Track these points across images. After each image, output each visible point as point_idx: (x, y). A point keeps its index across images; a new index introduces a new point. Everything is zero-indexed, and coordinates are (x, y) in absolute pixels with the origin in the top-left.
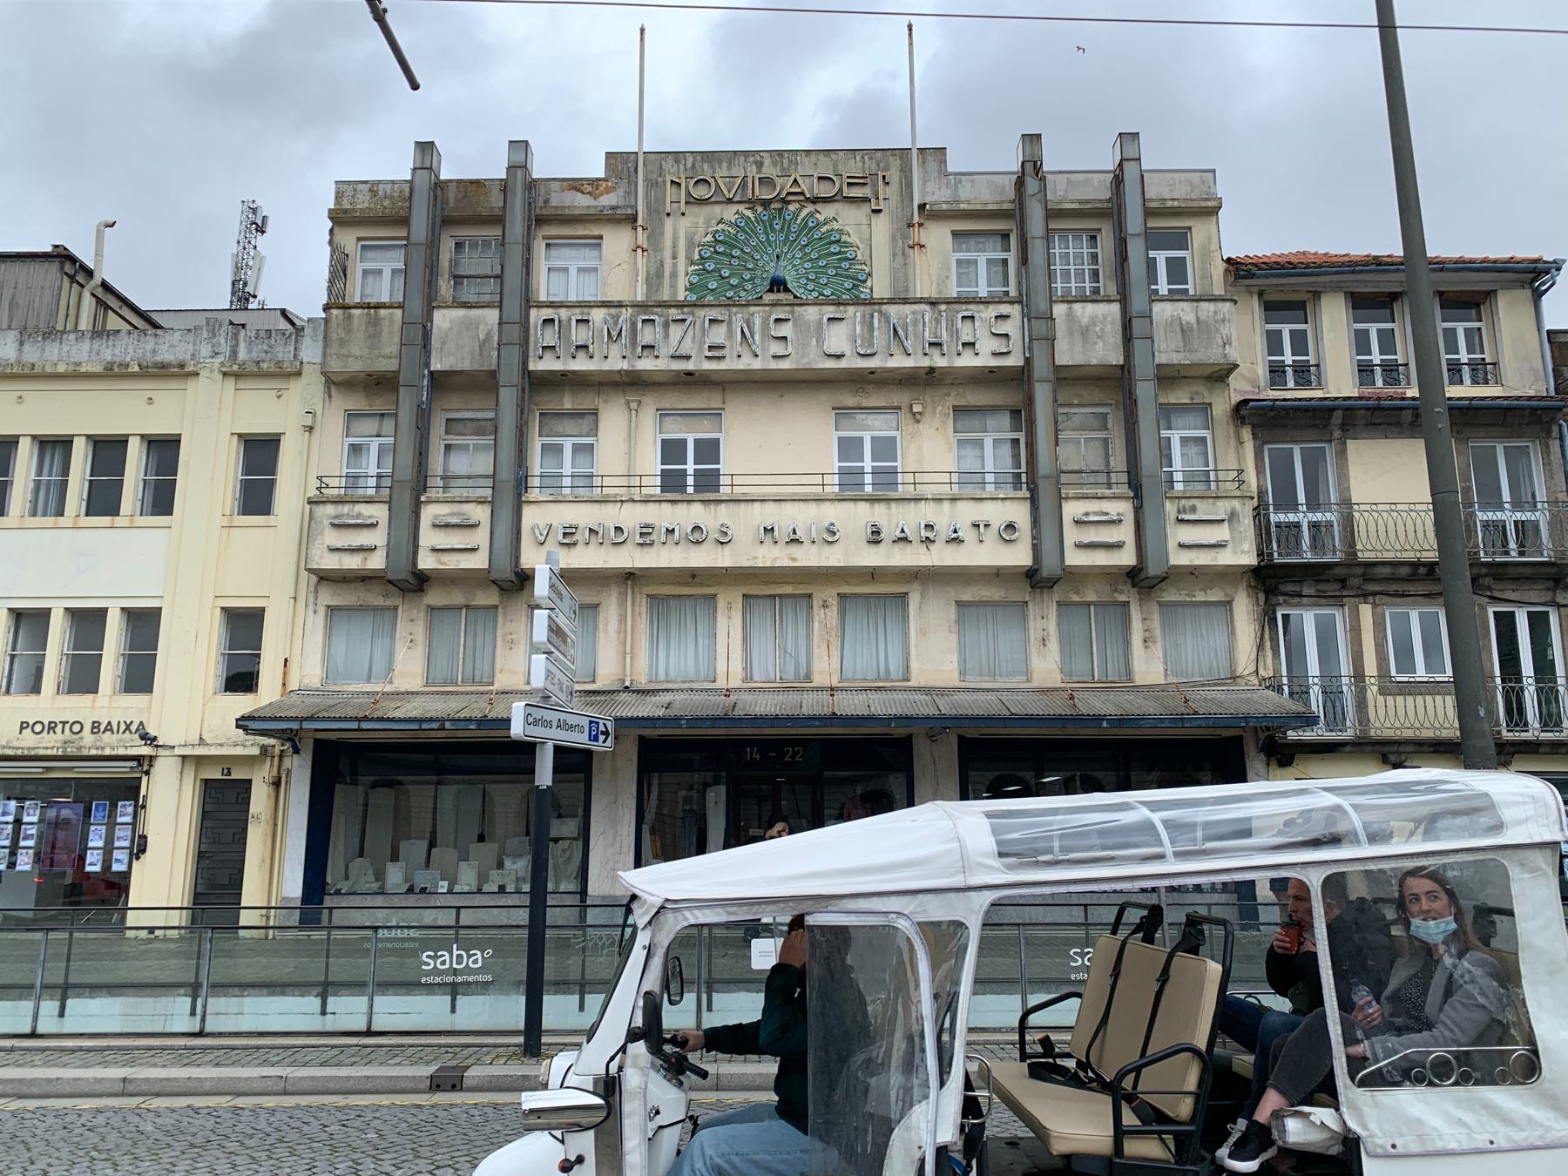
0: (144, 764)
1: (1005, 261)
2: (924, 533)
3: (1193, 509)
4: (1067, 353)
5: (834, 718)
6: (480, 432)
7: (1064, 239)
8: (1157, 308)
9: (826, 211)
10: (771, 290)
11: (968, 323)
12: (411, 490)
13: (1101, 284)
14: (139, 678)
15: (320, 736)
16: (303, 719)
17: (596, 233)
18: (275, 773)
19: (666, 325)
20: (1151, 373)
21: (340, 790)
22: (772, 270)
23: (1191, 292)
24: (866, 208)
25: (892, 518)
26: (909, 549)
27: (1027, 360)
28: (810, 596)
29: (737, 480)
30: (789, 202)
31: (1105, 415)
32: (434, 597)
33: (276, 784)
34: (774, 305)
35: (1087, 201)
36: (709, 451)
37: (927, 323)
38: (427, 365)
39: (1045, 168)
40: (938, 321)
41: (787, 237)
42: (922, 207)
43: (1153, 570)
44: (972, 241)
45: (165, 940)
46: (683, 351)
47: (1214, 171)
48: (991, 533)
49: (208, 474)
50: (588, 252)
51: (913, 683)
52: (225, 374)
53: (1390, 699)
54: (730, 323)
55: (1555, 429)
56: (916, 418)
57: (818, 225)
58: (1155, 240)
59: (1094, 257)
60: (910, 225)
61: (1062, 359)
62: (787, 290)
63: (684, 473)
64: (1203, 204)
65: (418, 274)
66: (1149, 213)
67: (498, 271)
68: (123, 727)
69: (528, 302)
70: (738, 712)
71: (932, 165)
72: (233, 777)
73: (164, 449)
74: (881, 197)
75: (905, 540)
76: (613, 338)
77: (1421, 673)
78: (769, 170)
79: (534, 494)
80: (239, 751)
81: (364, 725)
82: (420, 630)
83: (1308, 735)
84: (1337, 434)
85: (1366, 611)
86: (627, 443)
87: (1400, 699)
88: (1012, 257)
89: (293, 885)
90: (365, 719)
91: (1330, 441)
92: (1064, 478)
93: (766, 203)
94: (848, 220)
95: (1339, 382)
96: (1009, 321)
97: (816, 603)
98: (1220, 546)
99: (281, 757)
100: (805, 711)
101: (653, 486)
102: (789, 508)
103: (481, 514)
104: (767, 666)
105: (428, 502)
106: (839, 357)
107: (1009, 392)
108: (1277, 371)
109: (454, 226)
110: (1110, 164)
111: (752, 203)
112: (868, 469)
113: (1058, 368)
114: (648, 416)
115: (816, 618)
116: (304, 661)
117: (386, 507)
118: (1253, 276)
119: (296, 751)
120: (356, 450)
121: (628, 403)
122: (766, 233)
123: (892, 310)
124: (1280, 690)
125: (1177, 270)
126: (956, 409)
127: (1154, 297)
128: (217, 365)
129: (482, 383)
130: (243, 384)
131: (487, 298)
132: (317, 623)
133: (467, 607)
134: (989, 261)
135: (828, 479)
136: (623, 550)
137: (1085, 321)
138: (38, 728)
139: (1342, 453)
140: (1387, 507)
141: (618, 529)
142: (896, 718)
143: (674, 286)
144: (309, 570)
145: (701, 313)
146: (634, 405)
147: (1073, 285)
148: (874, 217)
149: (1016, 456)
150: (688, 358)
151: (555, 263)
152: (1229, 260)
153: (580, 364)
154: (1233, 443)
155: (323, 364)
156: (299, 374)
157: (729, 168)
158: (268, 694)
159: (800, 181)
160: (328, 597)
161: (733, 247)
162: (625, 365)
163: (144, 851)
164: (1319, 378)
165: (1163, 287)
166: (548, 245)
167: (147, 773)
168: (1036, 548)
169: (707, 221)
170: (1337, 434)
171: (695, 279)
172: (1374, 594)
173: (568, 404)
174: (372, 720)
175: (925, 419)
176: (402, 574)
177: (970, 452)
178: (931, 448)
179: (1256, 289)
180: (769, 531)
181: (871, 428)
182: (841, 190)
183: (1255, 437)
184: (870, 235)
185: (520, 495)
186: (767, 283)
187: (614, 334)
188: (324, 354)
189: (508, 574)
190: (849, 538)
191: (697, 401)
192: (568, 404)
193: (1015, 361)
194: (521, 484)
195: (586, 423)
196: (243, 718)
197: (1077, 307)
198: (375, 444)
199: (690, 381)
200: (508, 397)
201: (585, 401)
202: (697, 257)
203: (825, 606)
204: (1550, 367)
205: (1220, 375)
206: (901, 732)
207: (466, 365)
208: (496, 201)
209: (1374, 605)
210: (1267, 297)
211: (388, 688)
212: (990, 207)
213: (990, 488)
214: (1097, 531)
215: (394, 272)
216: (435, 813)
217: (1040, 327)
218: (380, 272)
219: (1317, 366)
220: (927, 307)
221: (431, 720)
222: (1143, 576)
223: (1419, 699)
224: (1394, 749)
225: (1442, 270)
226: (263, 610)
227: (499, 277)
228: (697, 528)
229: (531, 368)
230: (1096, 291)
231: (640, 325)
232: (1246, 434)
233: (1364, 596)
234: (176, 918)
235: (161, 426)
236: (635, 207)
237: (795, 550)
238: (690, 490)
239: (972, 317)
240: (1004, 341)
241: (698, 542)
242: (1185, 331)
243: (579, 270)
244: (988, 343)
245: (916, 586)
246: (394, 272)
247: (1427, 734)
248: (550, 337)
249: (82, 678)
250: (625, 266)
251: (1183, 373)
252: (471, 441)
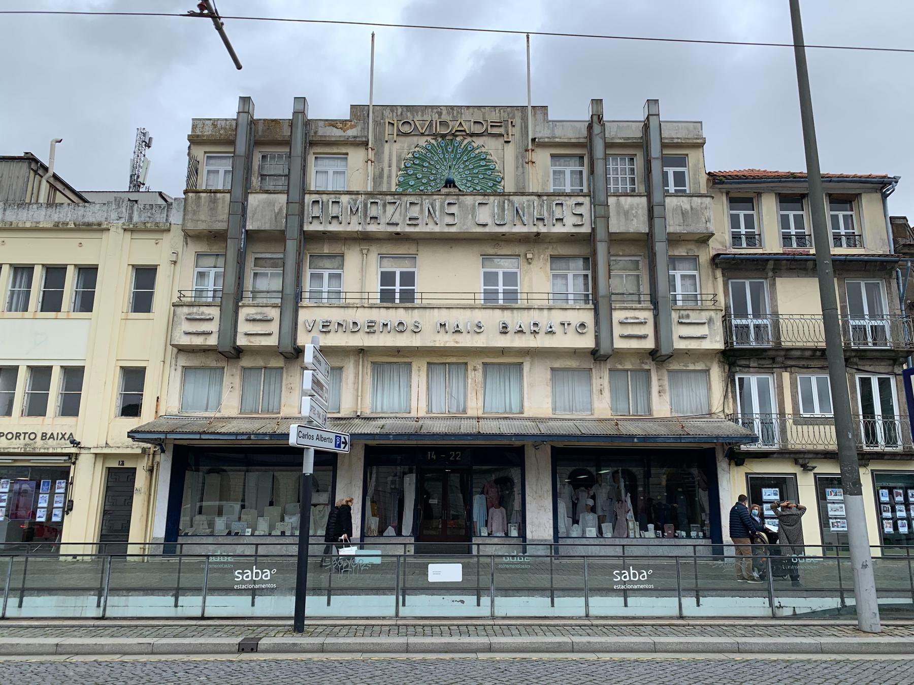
0: (72, 458)
1: (581, 172)
2: (533, 328)
3: (688, 316)
4: (616, 225)
5: (479, 435)
6: (275, 266)
7: (615, 159)
8: (668, 200)
9: (478, 142)
10: (446, 186)
11: (559, 207)
12: (233, 300)
13: (636, 186)
14: (71, 407)
15: (177, 442)
16: (166, 433)
17: (344, 151)
18: (150, 464)
19: (384, 206)
20: (664, 237)
21: (188, 474)
22: (446, 174)
23: (688, 192)
24: (501, 140)
25: (514, 319)
26: (524, 337)
27: (593, 229)
28: (466, 364)
29: (424, 296)
30: (457, 136)
31: (638, 261)
32: (246, 362)
33: (151, 471)
34: (448, 195)
35: (629, 138)
36: (408, 278)
37: (535, 207)
38: (244, 226)
39: (604, 119)
40: (542, 206)
41: (455, 156)
42: (533, 140)
43: (664, 351)
44: (562, 160)
45: (83, 562)
46: (394, 221)
47: (701, 123)
48: (571, 329)
49: (114, 288)
50: (339, 162)
51: (525, 415)
52: (125, 230)
53: (799, 427)
54: (422, 205)
55: (894, 273)
56: (529, 262)
57: (473, 149)
58: (667, 161)
59: (632, 170)
60: (527, 150)
61: (613, 229)
62: (455, 186)
63: (394, 291)
64: (695, 141)
65: (240, 173)
66: (664, 146)
67: (286, 172)
68: (60, 436)
69: (304, 191)
70: (423, 431)
71: (540, 116)
72: (125, 466)
73: (88, 273)
74: (510, 134)
75: (521, 332)
76: (354, 212)
77: (817, 412)
78: (445, 117)
79: (305, 302)
80: (129, 451)
81: (203, 437)
82: (237, 381)
83: (753, 448)
84: (770, 274)
85: (786, 376)
86: (361, 274)
87: (805, 427)
88: (585, 170)
89: (159, 530)
90: (204, 433)
91: (766, 278)
92: (614, 298)
93: (443, 136)
94: (491, 146)
95: (772, 245)
96: (583, 207)
97: (470, 368)
98: (703, 338)
99: (154, 455)
100: (463, 430)
101: (376, 298)
102: (454, 312)
103: (274, 313)
104: (441, 405)
105: (244, 306)
106: (485, 225)
107: (582, 247)
108: (736, 238)
109: (261, 146)
110: (642, 118)
111: (435, 136)
112: (501, 290)
113: (610, 234)
114: (373, 257)
115: (470, 376)
116: (168, 398)
117: (219, 308)
118: (723, 183)
119: (163, 451)
120: (201, 275)
121: (361, 250)
122: (443, 153)
123: (515, 199)
124: (736, 421)
125: (680, 179)
126: (552, 257)
127: (666, 194)
128: (120, 224)
129: (276, 237)
130: (135, 236)
131: (280, 188)
132: (177, 376)
133: (265, 367)
134: (572, 172)
135: (477, 296)
136: (358, 335)
137: (627, 207)
138: (10, 436)
139: (773, 285)
140: (798, 317)
141: (355, 323)
142: (516, 435)
143: (389, 183)
144: (173, 345)
145: (405, 199)
146: (365, 252)
147: (620, 186)
148: (506, 145)
149: (586, 284)
150: (397, 224)
151: (319, 169)
152: (709, 174)
153: (334, 227)
154: (711, 278)
155: (183, 225)
156: (169, 230)
157: (422, 116)
158: (147, 417)
159: (463, 124)
160: (183, 361)
161: (424, 161)
162: (360, 228)
163: (71, 510)
164: (760, 242)
165: (672, 188)
166: (316, 158)
167: (74, 463)
168: (597, 338)
169: (409, 147)
170: (770, 274)
171: (402, 179)
172: (791, 366)
173: (326, 250)
174: (208, 433)
175: (534, 262)
176: (227, 348)
177: (559, 281)
178: (537, 279)
179: (724, 190)
180: (443, 325)
181: (503, 267)
182: (487, 129)
183: (723, 275)
184: (503, 156)
185: (297, 303)
186: (443, 182)
187: (354, 210)
188: (184, 219)
189: (290, 349)
190: (489, 330)
191: (402, 250)
192: (326, 250)
193: (586, 229)
194: (298, 296)
195: (337, 261)
196: (132, 432)
197: (622, 199)
198: (213, 272)
199: (398, 238)
200: (291, 246)
201: (336, 249)
202: (403, 166)
203: (475, 370)
204: (891, 237)
205: (704, 239)
206: (517, 443)
207: (267, 227)
208: (286, 132)
209: (791, 373)
210: (731, 195)
211: (218, 415)
212: (573, 141)
213: (571, 302)
214: (632, 328)
215: (226, 172)
216: (244, 488)
217: (601, 210)
218: (218, 172)
219: (759, 235)
220: (536, 198)
221: (243, 434)
222: (658, 354)
223: (816, 427)
224: (802, 456)
225: (830, 181)
226: (145, 368)
227: (288, 176)
228: (401, 323)
229: (305, 228)
230: (633, 190)
231: (369, 205)
232: (719, 273)
233: (786, 368)
234: (89, 550)
236: (367, 137)
237: (458, 337)
238: (397, 301)
239: (562, 204)
240: (579, 218)
241: (401, 332)
242: (684, 214)
243: (335, 173)
244: (570, 219)
245: (528, 359)
246: (226, 172)
247: (820, 448)
248: (316, 211)
249: (37, 407)
250: (361, 171)
251: (682, 238)
252: (269, 271)
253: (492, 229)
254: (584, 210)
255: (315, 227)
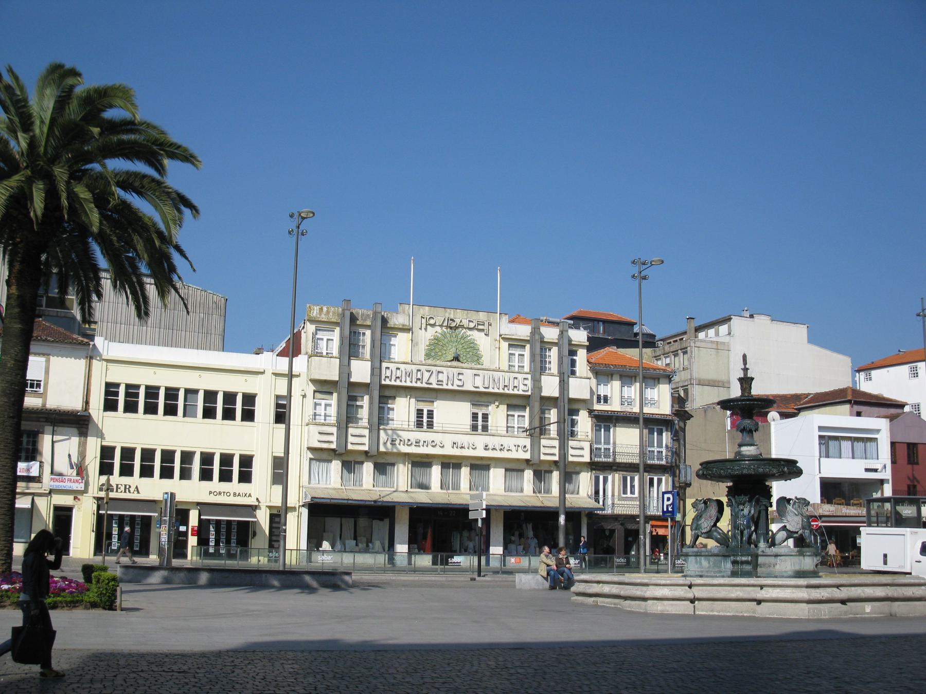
4: (545, 393)
9: (469, 333)
14: (245, 477)
24: (483, 334)
46: (430, 381)
48: (518, 447)
76: (409, 375)
93: (451, 328)
94: (476, 336)
111: (447, 327)
233: (616, 470)
235: (249, 390)
249: (206, 475)
253: (482, 389)
254: (529, 382)
255: (387, 382)
